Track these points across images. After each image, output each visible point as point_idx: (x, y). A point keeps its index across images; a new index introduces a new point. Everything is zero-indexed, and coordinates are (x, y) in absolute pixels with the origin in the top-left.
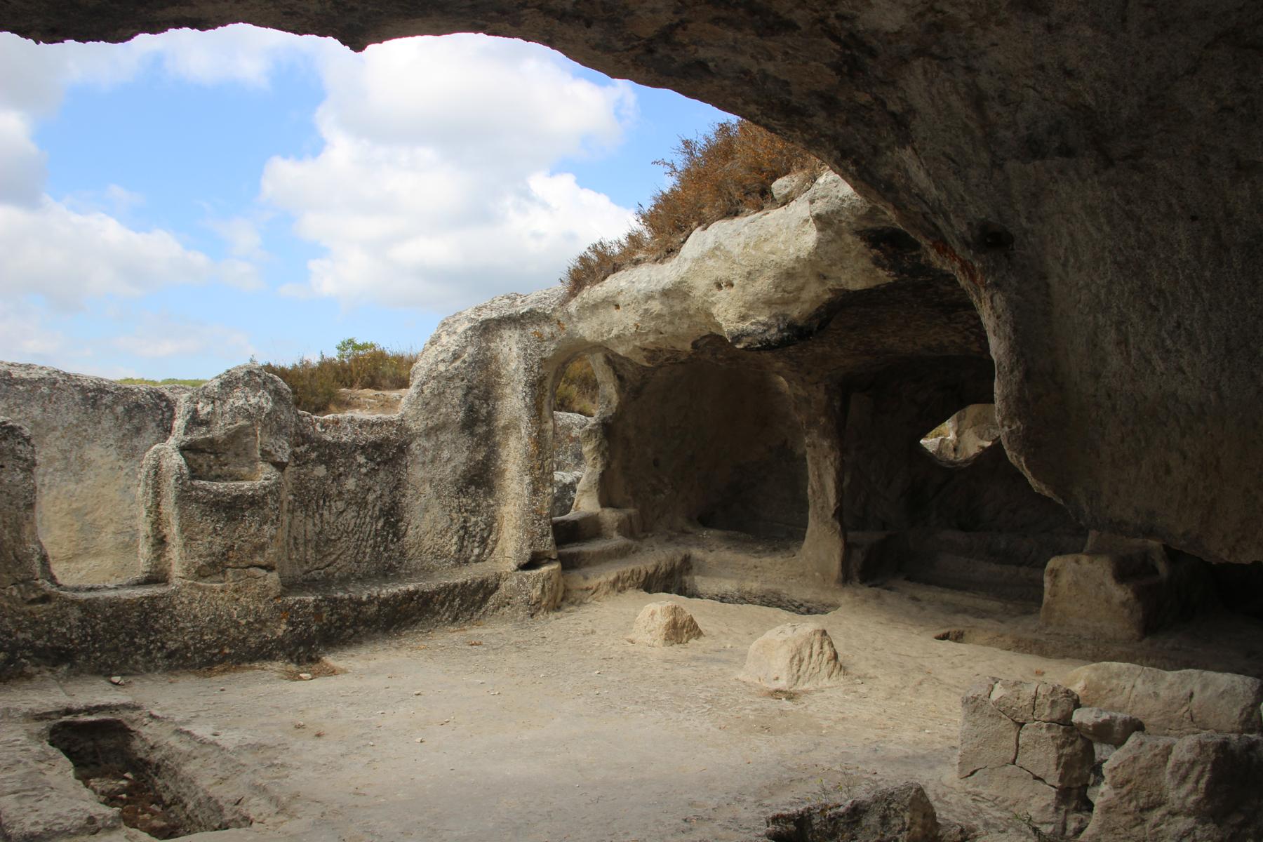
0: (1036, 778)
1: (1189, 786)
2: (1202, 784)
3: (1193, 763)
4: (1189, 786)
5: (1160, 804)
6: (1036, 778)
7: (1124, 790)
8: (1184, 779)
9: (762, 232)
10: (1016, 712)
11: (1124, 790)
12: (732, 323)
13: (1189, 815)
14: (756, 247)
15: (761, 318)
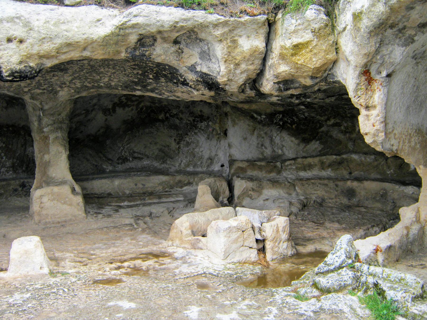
0: (250, 248)
1: (285, 233)
2: (288, 231)
3: (286, 226)
4: (285, 233)
5: (281, 241)
6: (250, 248)
7: (274, 241)
8: (284, 231)
9: (62, 18)
10: (243, 227)
11: (274, 241)
12: (13, 64)
13: (286, 241)
14: (55, 25)
15: (31, 64)
